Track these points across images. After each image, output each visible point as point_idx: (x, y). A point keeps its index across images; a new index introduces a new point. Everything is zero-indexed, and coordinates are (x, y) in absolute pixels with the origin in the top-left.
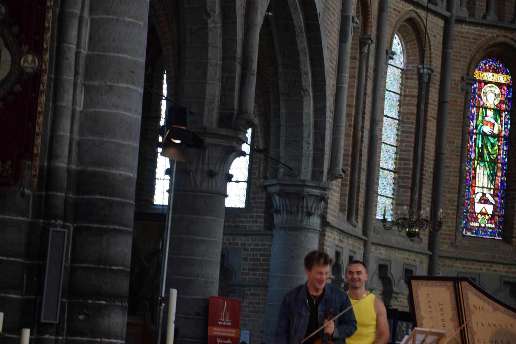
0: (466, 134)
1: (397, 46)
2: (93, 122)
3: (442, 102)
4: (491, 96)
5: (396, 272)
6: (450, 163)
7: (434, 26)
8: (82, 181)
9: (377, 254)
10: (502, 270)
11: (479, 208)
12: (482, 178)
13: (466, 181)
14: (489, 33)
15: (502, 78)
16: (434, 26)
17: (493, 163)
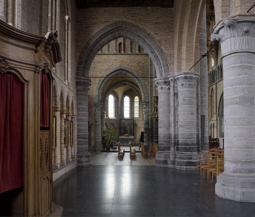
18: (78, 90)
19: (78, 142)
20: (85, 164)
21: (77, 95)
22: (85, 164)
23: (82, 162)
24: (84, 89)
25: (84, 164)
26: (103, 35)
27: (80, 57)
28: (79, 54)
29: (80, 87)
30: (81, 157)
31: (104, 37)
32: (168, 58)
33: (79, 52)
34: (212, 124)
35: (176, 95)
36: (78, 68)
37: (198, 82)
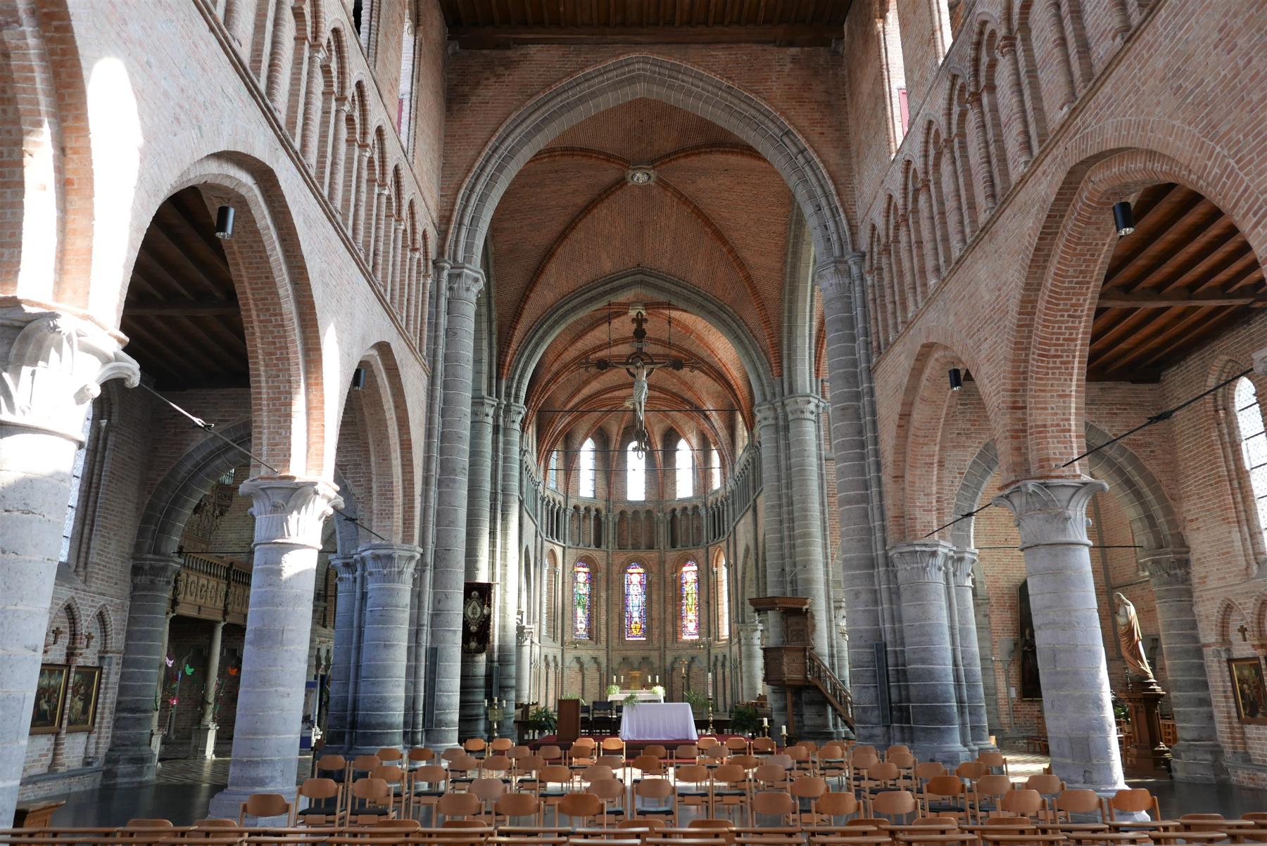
0: (573, 595)
1: (546, 561)
2: (503, 628)
3: (563, 583)
4: (582, 577)
5: (550, 658)
6: (568, 608)
7: (559, 551)
8: (502, 648)
9: (545, 651)
10: (591, 652)
11: (579, 626)
12: (580, 612)
13: (574, 615)
14: (580, 552)
15: (586, 570)
16: (559, 551)
17: (584, 606)
18: (135, 587)
19: (117, 720)
20: (125, 780)
21: (133, 598)
22: (125, 780)
23: (115, 776)
24: (152, 582)
25: (119, 780)
26: (213, 452)
27: (150, 503)
28: (149, 497)
29: (143, 580)
30: (116, 762)
31: (218, 456)
32: (360, 506)
33: (149, 493)
34: (720, 658)
35: (364, 596)
36: (141, 533)
37: (421, 568)
